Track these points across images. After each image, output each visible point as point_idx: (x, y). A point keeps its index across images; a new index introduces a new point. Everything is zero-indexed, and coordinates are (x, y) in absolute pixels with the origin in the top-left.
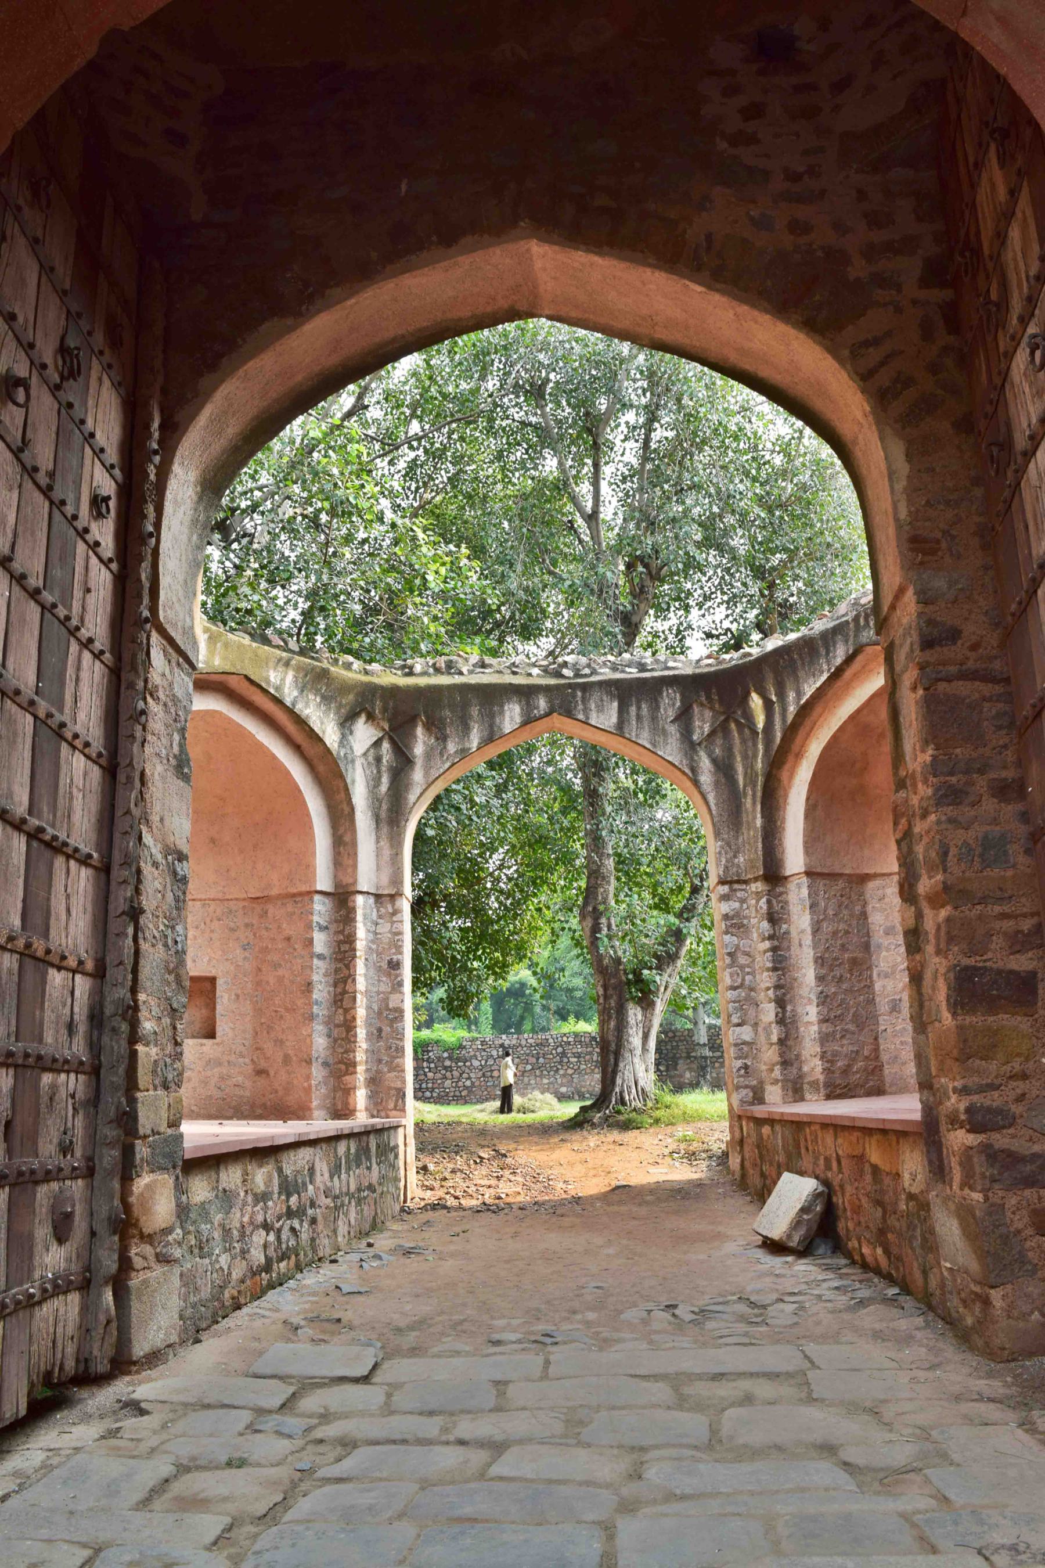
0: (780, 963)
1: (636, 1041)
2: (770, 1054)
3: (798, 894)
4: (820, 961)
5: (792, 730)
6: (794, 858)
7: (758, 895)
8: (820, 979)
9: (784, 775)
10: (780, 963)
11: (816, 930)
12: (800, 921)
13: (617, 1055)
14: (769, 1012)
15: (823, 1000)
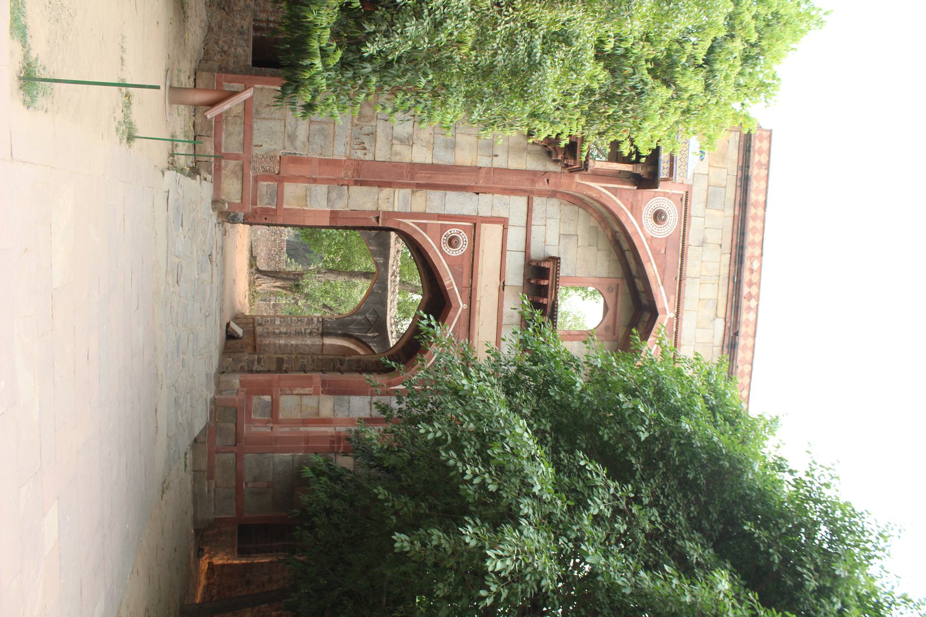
0: (299, 334)
1: (278, 284)
2: (271, 329)
3: (317, 341)
4: (297, 345)
5: (364, 343)
6: (328, 341)
7: (318, 329)
8: (292, 345)
9: (353, 340)
10: (299, 334)
11: (307, 345)
12: (309, 342)
13: (274, 277)
14: (283, 330)
15: (286, 345)
